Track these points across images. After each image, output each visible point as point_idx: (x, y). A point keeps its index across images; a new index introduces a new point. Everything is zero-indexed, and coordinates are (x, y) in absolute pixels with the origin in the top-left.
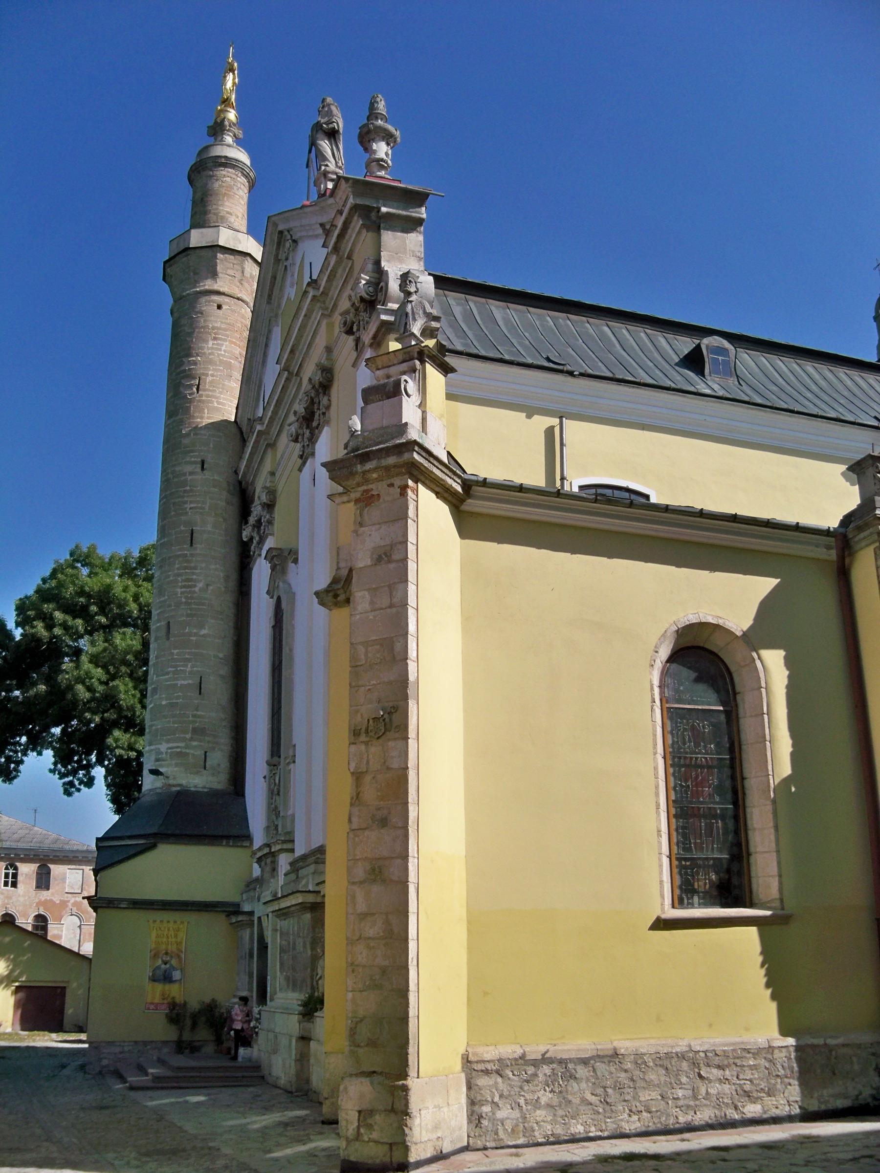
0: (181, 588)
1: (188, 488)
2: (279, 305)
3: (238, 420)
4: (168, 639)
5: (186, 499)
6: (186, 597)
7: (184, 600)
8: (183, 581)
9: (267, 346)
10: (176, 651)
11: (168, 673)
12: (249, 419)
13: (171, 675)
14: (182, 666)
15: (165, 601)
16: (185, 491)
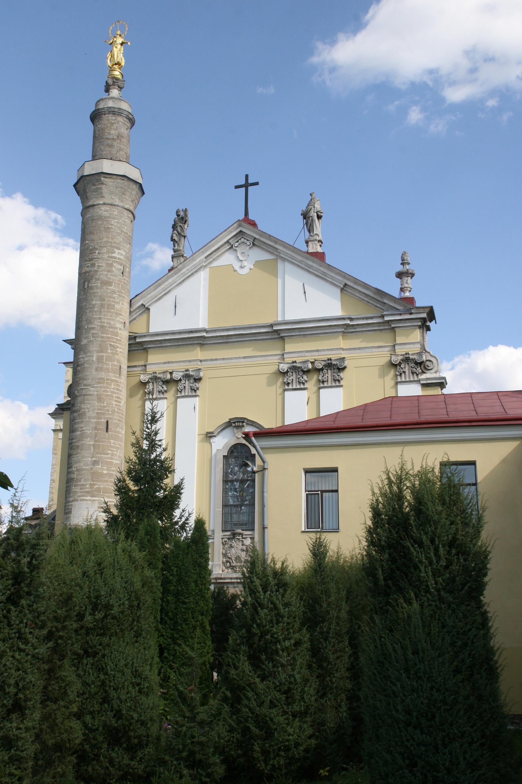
0: (116, 401)
1: (119, 338)
2: (210, 263)
3: (133, 301)
4: (107, 431)
5: (117, 345)
6: (117, 408)
7: (116, 410)
8: (116, 397)
9: (188, 277)
10: (112, 441)
11: (108, 454)
12: (143, 305)
13: (110, 456)
14: (116, 451)
15: (104, 407)
16: (117, 339)
